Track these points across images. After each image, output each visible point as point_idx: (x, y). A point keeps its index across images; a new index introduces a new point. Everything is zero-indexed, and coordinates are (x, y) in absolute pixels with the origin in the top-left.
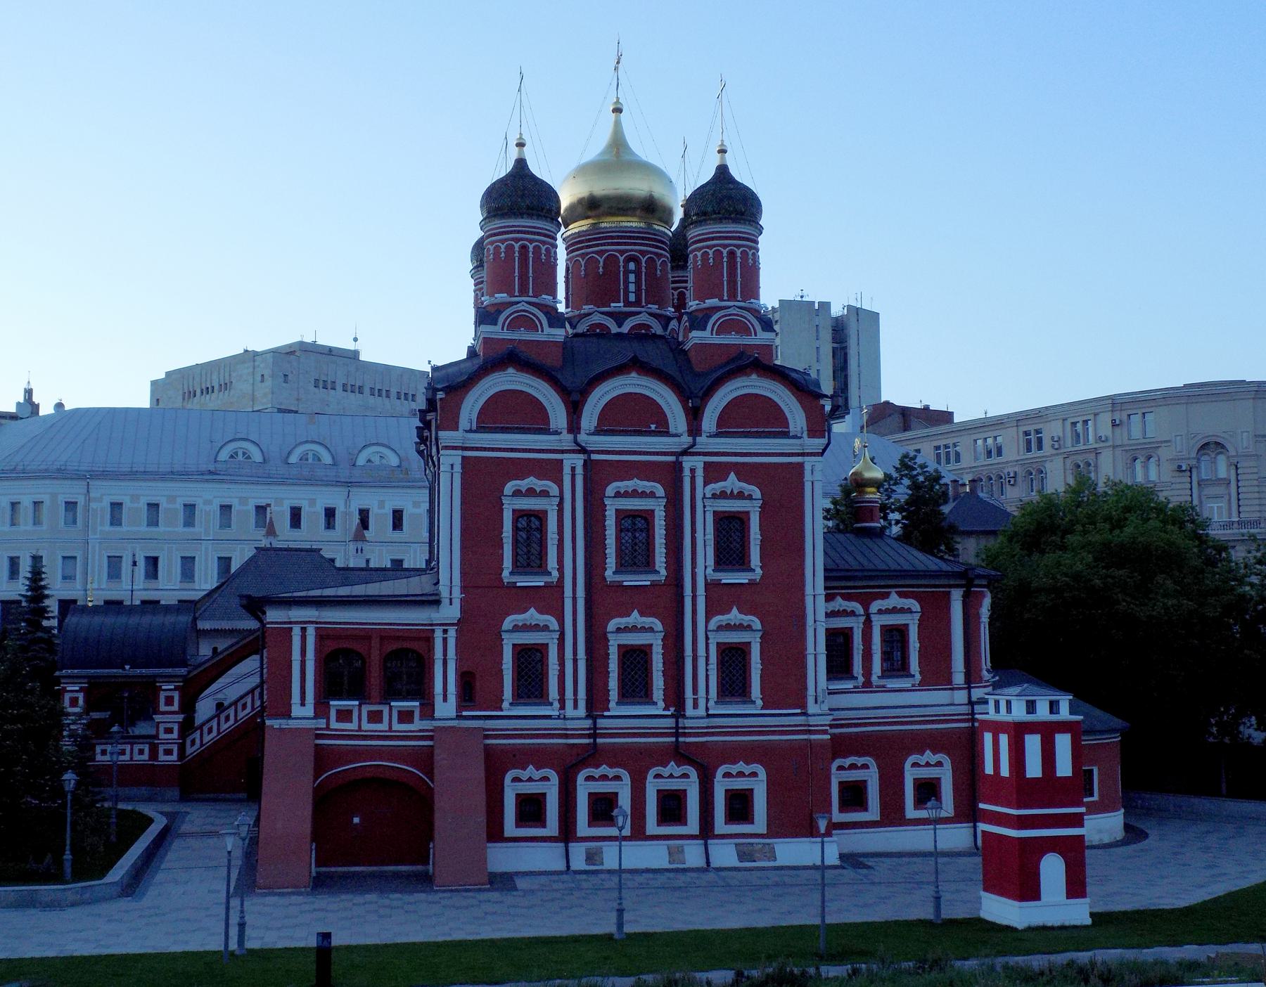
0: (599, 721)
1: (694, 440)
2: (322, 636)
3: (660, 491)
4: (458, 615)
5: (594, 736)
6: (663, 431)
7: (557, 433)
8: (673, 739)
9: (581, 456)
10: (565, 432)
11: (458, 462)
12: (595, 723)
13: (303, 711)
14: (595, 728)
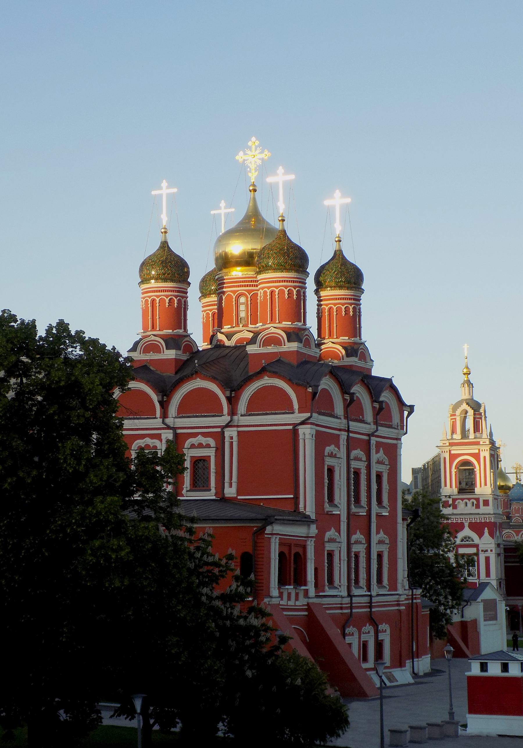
0: (353, 598)
1: (377, 428)
2: (282, 544)
3: (364, 459)
4: (317, 531)
5: (351, 608)
6: (362, 421)
7: (337, 417)
8: (369, 610)
9: (346, 433)
10: (342, 417)
11: (314, 432)
12: (351, 600)
13: (275, 592)
14: (351, 603)
